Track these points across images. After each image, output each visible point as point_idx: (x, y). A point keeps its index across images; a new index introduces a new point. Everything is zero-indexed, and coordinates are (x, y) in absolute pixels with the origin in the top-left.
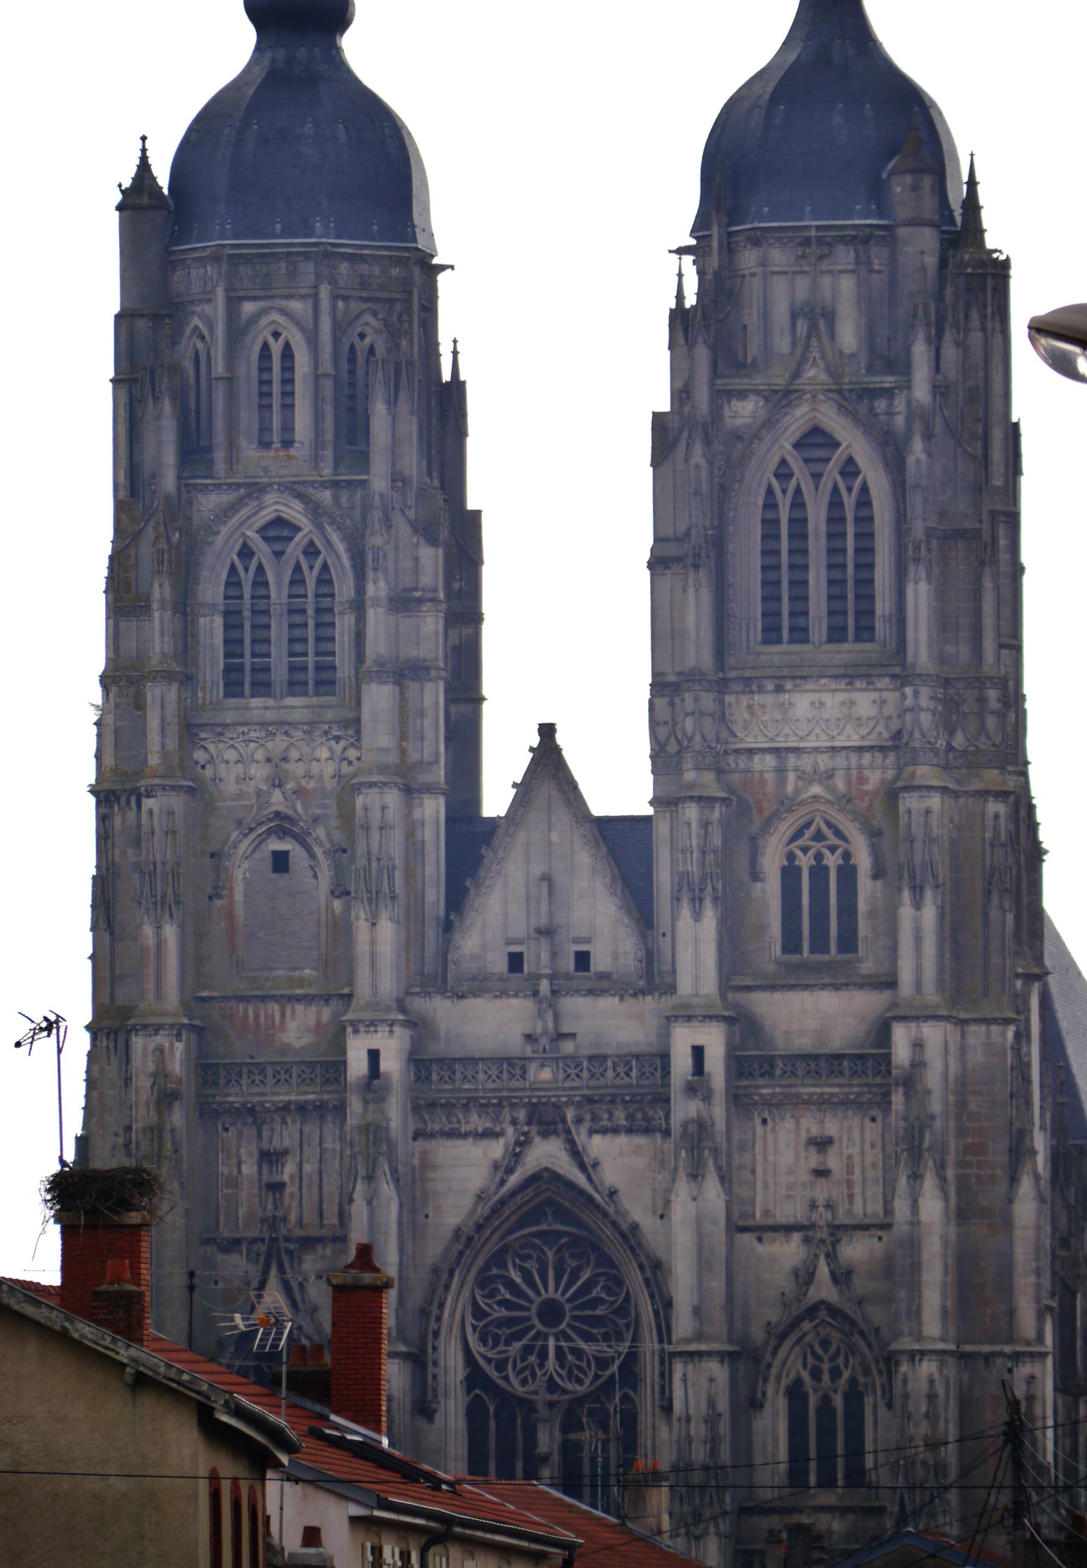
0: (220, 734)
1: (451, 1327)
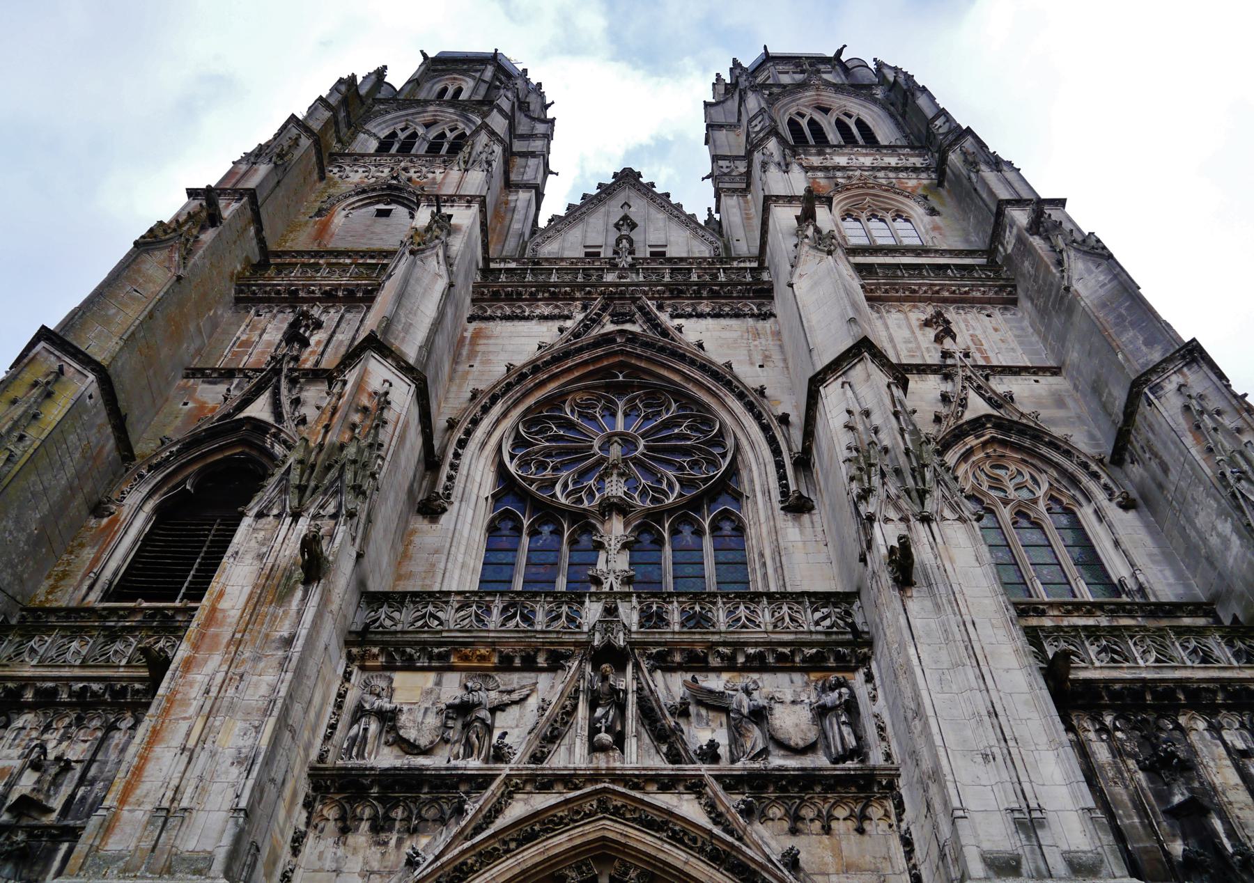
0: (356, 160)
1: (483, 445)
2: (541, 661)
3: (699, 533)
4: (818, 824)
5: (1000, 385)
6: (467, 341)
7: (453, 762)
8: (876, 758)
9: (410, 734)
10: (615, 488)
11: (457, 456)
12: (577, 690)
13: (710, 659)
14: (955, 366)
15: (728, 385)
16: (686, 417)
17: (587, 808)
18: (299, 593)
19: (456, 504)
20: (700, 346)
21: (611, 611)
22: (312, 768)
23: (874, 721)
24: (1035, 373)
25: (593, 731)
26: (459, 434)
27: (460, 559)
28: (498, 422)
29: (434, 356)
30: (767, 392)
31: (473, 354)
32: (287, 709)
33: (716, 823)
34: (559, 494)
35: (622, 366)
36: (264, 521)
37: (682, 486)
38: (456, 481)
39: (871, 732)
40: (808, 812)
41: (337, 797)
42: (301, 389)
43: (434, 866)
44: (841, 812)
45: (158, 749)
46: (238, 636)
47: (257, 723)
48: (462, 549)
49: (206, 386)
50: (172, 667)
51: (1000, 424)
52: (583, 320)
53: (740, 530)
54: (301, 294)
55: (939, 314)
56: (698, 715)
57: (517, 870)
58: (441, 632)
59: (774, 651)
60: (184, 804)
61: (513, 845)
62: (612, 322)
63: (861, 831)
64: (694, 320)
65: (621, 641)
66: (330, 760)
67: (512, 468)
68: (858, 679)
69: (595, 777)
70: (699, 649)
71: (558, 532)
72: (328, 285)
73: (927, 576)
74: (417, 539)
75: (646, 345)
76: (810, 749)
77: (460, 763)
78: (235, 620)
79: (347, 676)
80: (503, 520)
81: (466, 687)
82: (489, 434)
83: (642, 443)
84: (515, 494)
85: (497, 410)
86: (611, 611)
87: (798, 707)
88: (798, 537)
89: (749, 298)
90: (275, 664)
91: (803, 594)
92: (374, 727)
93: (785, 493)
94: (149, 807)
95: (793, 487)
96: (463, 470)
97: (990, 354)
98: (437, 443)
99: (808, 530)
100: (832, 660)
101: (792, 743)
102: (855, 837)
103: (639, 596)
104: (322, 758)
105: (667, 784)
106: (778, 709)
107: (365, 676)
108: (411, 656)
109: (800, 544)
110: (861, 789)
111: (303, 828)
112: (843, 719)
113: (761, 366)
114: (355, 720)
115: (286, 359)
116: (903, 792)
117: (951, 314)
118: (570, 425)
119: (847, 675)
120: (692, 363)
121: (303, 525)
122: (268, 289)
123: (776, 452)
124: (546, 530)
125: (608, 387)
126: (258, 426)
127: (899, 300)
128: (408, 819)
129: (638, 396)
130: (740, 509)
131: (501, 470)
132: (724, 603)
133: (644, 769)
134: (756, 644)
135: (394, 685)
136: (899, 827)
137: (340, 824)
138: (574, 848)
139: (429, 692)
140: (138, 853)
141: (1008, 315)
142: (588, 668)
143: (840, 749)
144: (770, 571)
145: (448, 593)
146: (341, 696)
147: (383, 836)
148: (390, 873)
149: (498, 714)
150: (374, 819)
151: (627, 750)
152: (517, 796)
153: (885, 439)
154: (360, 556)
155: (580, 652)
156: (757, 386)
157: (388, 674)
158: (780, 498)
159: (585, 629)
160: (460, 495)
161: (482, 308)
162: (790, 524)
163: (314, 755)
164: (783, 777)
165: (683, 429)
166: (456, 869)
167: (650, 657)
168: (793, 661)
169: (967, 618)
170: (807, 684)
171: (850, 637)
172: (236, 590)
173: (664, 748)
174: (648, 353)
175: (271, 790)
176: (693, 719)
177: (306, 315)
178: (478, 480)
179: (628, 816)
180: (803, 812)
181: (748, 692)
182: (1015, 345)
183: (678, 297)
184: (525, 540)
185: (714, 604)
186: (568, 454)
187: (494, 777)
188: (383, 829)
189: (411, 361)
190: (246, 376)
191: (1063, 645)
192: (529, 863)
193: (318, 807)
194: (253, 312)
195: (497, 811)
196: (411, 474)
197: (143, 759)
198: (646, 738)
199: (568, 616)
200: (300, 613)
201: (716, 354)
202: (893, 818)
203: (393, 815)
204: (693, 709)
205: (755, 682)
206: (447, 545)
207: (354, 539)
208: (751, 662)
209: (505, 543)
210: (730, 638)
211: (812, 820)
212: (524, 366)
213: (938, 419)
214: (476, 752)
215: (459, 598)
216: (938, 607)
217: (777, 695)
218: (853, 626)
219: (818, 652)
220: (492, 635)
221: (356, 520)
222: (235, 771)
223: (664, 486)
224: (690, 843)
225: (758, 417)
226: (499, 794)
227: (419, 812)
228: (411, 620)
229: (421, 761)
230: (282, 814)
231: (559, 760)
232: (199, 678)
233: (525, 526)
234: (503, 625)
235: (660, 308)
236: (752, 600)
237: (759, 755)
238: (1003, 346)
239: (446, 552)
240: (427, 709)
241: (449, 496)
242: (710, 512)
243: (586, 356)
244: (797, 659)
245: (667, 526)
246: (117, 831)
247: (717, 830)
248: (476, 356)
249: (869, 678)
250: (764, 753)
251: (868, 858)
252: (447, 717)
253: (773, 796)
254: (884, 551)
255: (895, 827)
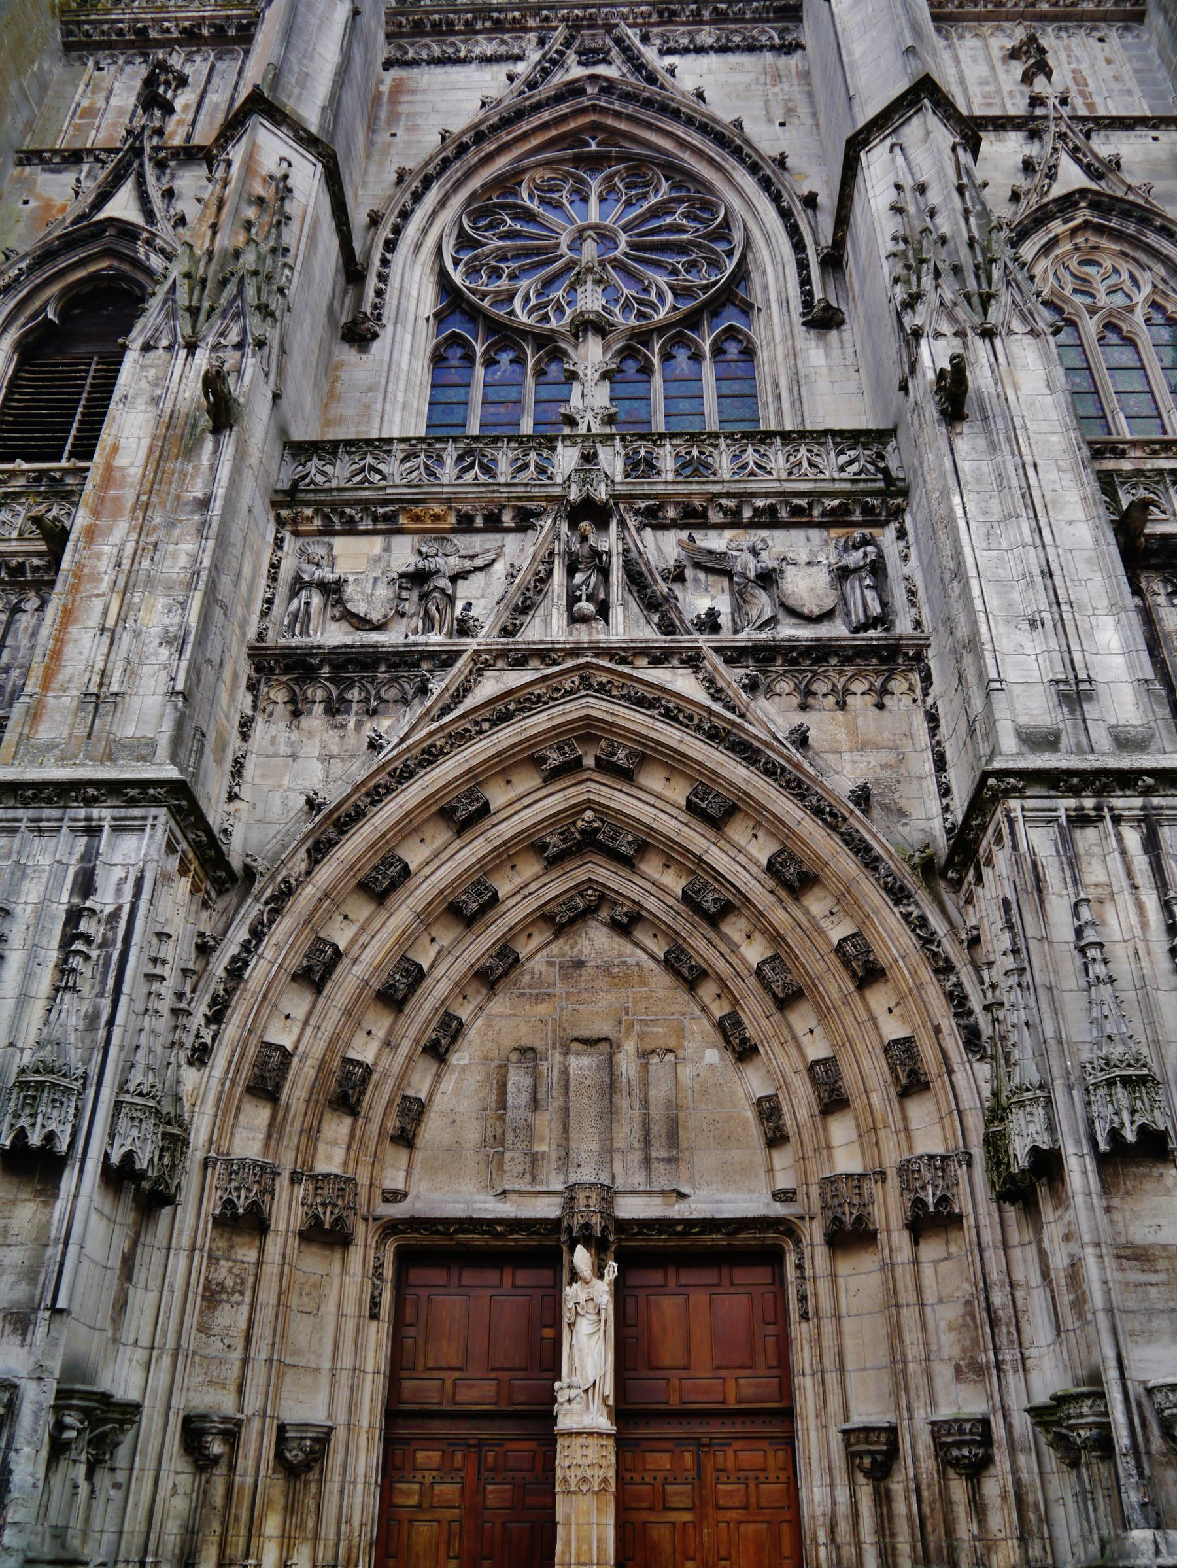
1: (418, 247)
2: (507, 519)
3: (697, 357)
4: (831, 699)
5: (1104, 146)
6: (385, 98)
7: (412, 638)
8: (903, 626)
9: (359, 607)
10: (590, 300)
11: (385, 262)
12: (551, 554)
13: (710, 514)
14: (1046, 117)
15: (737, 152)
16: (680, 200)
17: (568, 685)
18: (209, 444)
19: (390, 328)
20: (700, 96)
21: (589, 458)
22: (251, 648)
23: (903, 584)
24: (1155, 127)
25: (572, 600)
26: (385, 233)
27: (400, 398)
28: (434, 214)
29: (343, 122)
30: (789, 162)
31: (394, 117)
32: (214, 582)
33: (715, 699)
34: (518, 311)
35: (595, 128)
36: (152, 355)
37: (676, 295)
38: (387, 297)
39: (899, 597)
40: (820, 687)
41: (284, 678)
42: (173, 176)
43: (400, 748)
44: (859, 686)
45: (74, 631)
46: (144, 498)
47: (181, 599)
48: (402, 386)
49: (48, 176)
50: (73, 537)
51: (1100, 203)
52: (539, 62)
53: (749, 353)
54: (153, 34)
55: (1032, 39)
56: (696, 579)
57: (492, 752)
58: (385, 488)
59: (787, 503)
60: (115, 688)
61: (486, 726)
62: (580, 63)
63: (880, 706)
64: (691, 57)
65: (602, 493)
66: (270, 641)
67: (457, 276)
68: (887, 536)
69: (575, 652)
70: (697, 502)
71: (519, 361)
72: (187, 19)
73: (982, 407)
74: (344, 374)
75: (628, 97)
76: (827, 616)
77: (420, 638)
78: (137, 480)
79: (279, 543)
80: (450, 346)
81: (420, 553)
82: (425, 231)
83: (623, 238)
84: (464, 312)
85: (432, 197)
86: (589, 458)
87: (814, 569)
88: (823, 362)
89: (768, 21)
90: (192, 530)
91: (826, 433)
92: (316, 600)
93: (808, 304)
94: (76, 693)
95: (818, 295)
96: (395, 281)
97: (1097, 100)
98: (357, 246)
99: (836, 352)
100: (857, 513)
101: (806, 611)
102: (873, 713)
103: (623, 439)
104: (261, 637)
105: (659, 658)
106: (790, 571)
107: (300, 541)
108: (352, 517)
109: (825, 371)
110: (883, 660)
111: (249, 712)
112: (868, 582)
113: (782, 124)
114: (294, 593)
115: (147, 133)
116: (932, 664)
117: (1049, 39)
118: (528, 216)
119: (875, 531)
120: (689, 121)
121: (202, 359)
122: (106, 27)
123: (799, 246)
124: (505, 358)
125: (577, 161)
126: (127, 231)
127: (979, 18)
128: (367, 700)
129: (617, 172)
130: (749, 325)
131: (443, 280)
132: (728, 446)
133: (633, 641)
134: (767, 495)
135: (335, 552)
136: (924, 702)
137: (290, 707)
138: (555, 727)
139: (377, 559)
140: (73, 741)
141: (1129, 39)
142: (564, 527)
143: (861, 616)
144: (786, 405)
145: (390, 441)
146: (275, 566)
147: (340, 719)
148: (352, 757)
149: (460, 582)
150: (328, 701)
151: (612, 620)
152: (487, 673)
153: (944, 224)
154: (276, 397)
155: (552, 508)
156: (775, 154)
157: (326, 539)
158: (801, 310)
159: (559, 480)
160: (393, 316)
161: (400, 47)
162: (813, 344)
163: (252, 634)
164: (794, 648)
165: (676, 218)
166: (423, 752)
167: (637, 512)
168: (811, 515)
169: (1028, 459)
170: (826, 542)
171: (881, 485)
172: (133, 444)
173: (656, 618)
174: (630, 109)
175: (208, 673)
176: (689, 584)
177: (162, 66)
178: (414, 293)
179: (615, 692)
180: (815, 687)
181: (755, 552)
182: (1132, 84)
183: (670, 22)
184: (479, 371)
185: (716, 446)
186: (527, 255)
187: (459, 653)
188: (338, 711)
189: (314, 129)
190: (97, 160)
191: (1142, 493)
192: (505, 745)
193: (264, 689)
194: (91, 64)
195: (464, 690)
196: (329, 289)
197: (60, 641)
198: (634, 607)
199: (537, 466)
200: (213, 469)
201: (721, 109)
202: (919, 692)
203: (348, 696)
204: (689, 573)
205: (763, 540)
206: (383, 381)
207: (267, 375)
208: (760, 516)
209: (453, 376)
210: (735, 488)
211: (825, 695)
212: (464, 133)
213: (1015, 197)
214: (437, 626)
215: (403, 446)
216: (993, 446)
217: (790, 555)
218: (886, 471)
219: (841, 504)
220: (446, 490)
221: (266, 350)
222: (164, 652)
223: (653, 297)
224: (686, 721)
225: (776, 198)
226: (466, 672)
227: (378, 693)
228: (347, 474)
229: (375, 637)
230: (224, 698)
231: (533, 633)
232: (106, 549)
233: (478, 354)
234: (459, 478)
235: (645, 39)
236: (762, 441)
237: (766, 624)
238: (1116, 86)
239: (382, 390)
240: (376, 579)
241: (379, 317)
242: (711, 330)
243: (546, 116)
244: (816, 513)
245: (656, 349)
246: (45, 718)
247: (716, 707)
248: (398, 120)
249: (902, 534)
250: (772, 621)
251: (886, 735)
252: (400, 587)
253: (781, 669)
254: (931, 375)
255: (919, 702)
